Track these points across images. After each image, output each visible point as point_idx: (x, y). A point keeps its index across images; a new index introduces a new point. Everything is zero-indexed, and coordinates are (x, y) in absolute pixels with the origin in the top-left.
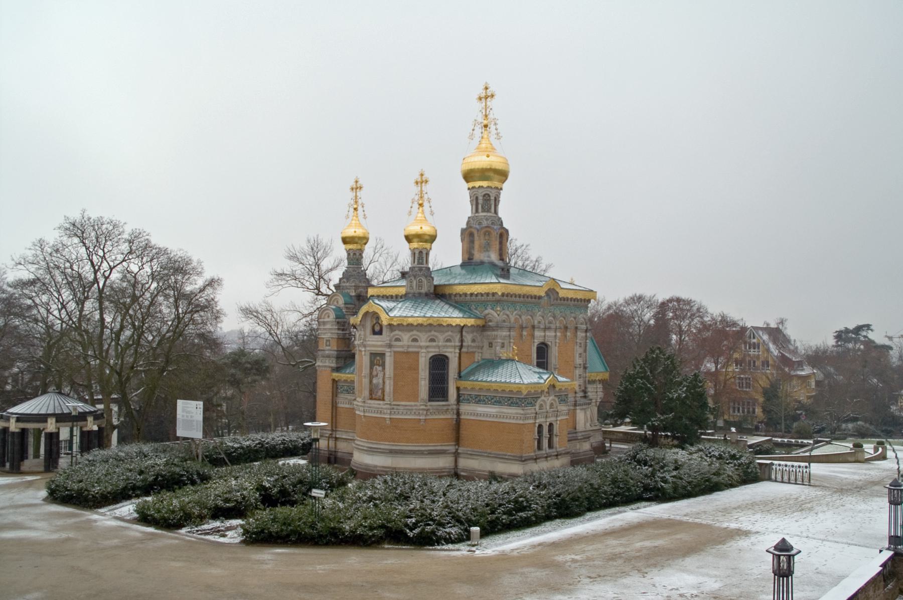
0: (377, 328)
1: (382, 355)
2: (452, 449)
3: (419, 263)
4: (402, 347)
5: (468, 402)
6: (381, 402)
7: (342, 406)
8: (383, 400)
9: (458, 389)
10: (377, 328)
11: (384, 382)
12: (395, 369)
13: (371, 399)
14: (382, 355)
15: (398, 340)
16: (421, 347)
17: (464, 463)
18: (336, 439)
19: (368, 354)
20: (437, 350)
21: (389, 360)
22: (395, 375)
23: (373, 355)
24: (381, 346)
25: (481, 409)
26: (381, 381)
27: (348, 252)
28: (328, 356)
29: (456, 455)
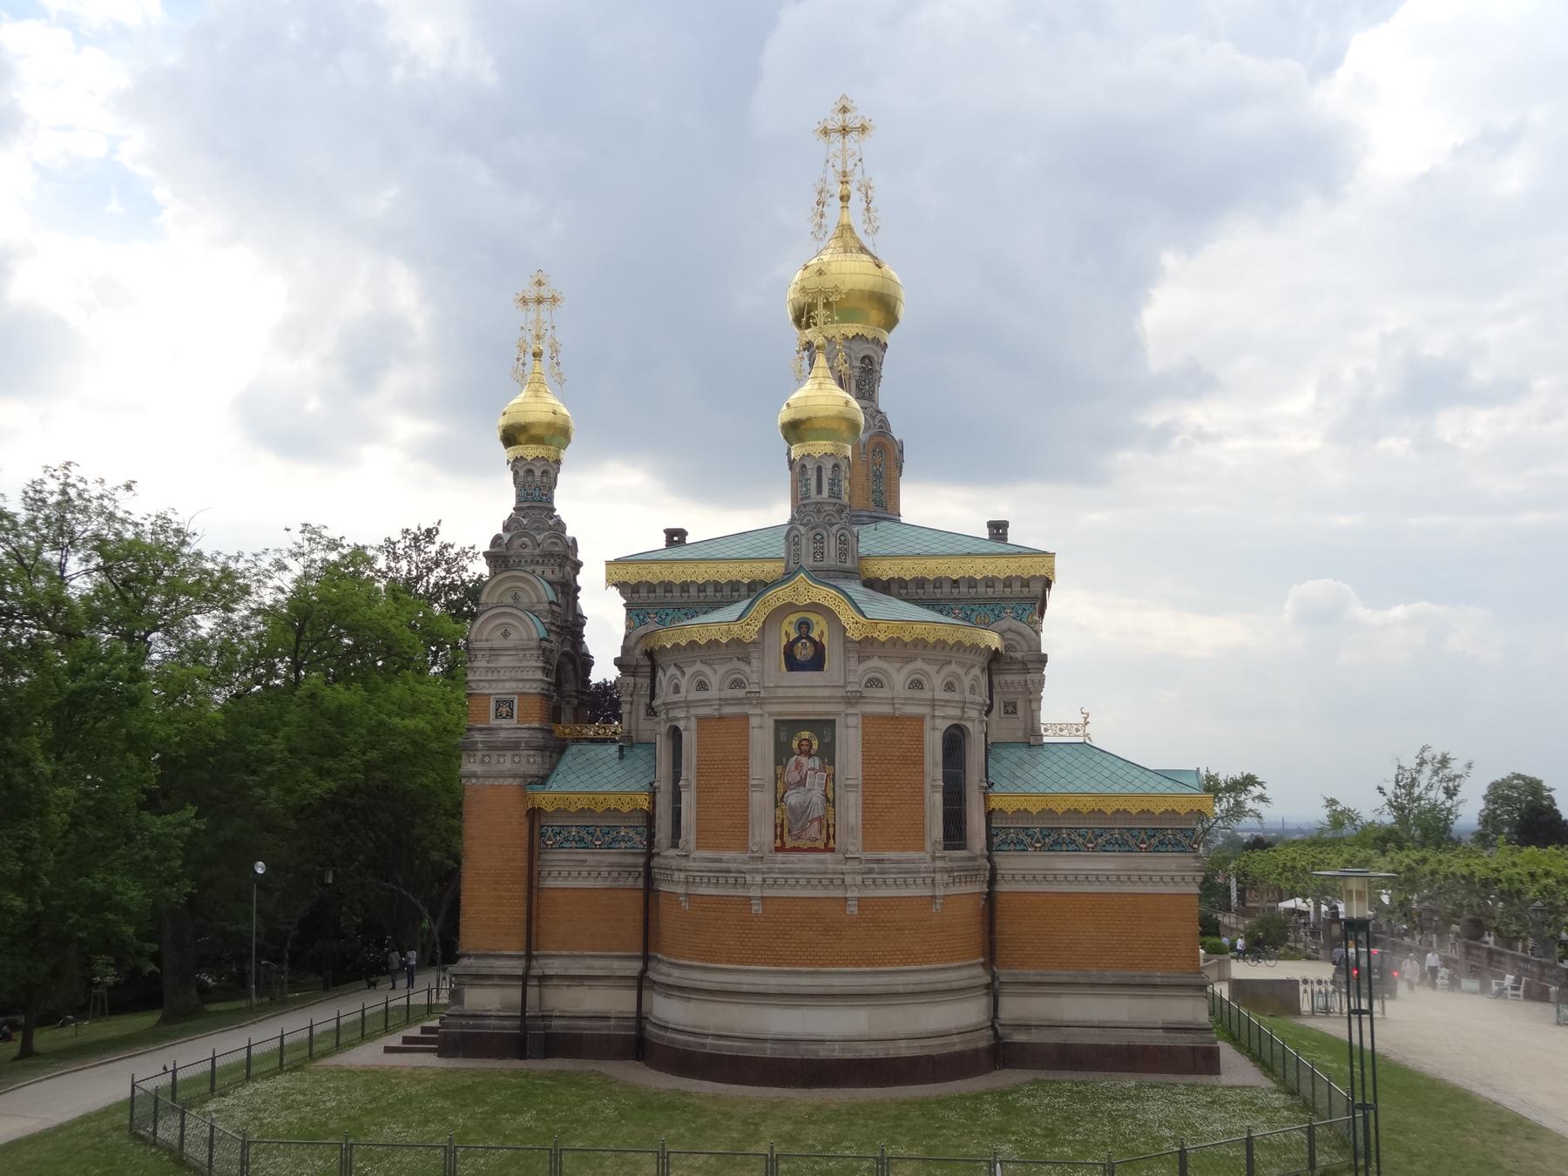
0: (804, 652)
1: (823, 727)
2: (980, 976)
3: (833, 494)
5: (1020, 846)
6: (828, 856)
7: (561, 883)
8: (828, 849)
9: (989, 815)
10: (804, 652)
11: (830, 802)
12: (866, 762)
13: (781, 849)
14: (823, 727)
15: (874, 683)
16: (933, 703)
17: (1014, 1007)
18: (543, 978)
20: (958, 713)
22: (866, 779)
23: (786, 728)
24: (828, 700)
26: (817, 797)
27: (516, 463)
28: (513, 746)
29: (993, 991)
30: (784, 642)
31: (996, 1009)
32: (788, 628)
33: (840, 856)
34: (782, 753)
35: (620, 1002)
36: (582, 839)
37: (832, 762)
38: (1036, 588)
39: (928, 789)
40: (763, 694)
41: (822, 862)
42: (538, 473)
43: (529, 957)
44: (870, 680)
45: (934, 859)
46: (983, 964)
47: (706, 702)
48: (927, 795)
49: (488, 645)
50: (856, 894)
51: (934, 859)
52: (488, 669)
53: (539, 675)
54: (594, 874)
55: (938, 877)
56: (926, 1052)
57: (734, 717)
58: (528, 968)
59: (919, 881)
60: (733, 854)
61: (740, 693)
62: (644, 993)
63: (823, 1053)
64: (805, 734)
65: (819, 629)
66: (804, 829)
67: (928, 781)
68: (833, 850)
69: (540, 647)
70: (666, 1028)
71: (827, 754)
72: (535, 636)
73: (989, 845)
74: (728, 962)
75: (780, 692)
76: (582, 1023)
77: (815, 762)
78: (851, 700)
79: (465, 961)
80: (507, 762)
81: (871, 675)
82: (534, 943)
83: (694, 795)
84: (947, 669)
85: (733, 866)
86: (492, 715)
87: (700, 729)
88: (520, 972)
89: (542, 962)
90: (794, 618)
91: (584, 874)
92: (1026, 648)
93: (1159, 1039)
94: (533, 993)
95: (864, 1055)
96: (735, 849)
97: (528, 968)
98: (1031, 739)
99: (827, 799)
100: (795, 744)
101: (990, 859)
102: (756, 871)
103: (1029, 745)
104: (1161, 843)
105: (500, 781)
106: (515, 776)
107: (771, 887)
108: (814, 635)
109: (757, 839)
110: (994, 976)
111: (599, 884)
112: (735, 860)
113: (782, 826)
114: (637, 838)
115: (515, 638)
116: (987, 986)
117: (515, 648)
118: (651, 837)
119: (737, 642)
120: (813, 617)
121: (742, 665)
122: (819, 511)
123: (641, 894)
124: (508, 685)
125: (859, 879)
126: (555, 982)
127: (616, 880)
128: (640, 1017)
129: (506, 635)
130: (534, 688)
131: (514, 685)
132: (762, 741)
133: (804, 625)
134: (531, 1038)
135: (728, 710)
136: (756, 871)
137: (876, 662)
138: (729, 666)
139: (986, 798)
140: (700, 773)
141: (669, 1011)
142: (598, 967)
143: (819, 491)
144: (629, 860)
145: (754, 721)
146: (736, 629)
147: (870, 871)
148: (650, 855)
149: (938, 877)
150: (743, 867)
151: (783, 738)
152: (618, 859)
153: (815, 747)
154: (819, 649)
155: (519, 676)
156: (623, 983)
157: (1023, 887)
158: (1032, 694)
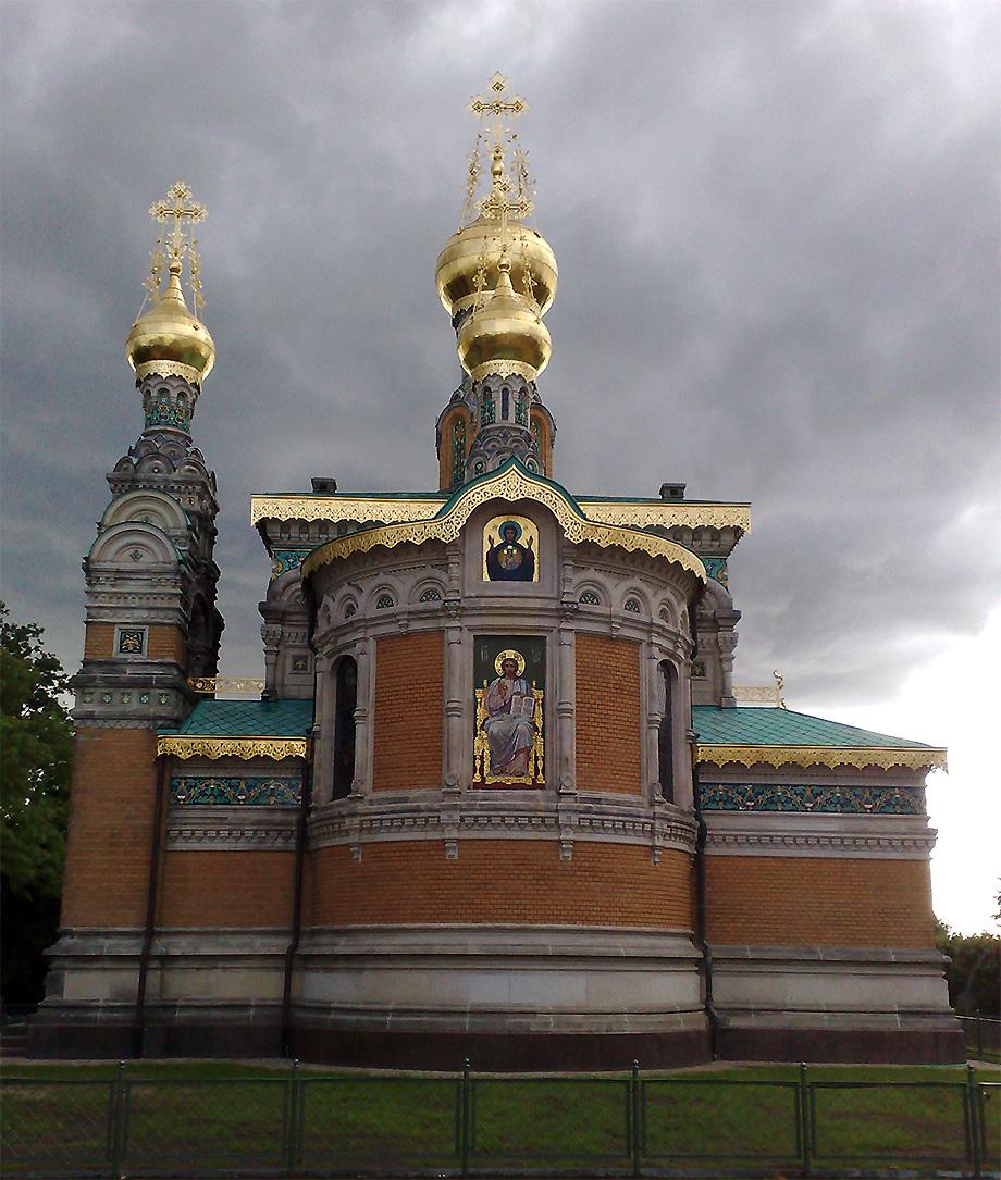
1: (532, 645)
4: (608, 619)
5: (730, 804)
7: (195, 846)
8: (535, 786)
9: (697, 769)
10: (510, 558)
14: (532, 645)
15: (589, 597)
16: (649, 628)
17: (728, 988)
18: (167, 960)
19: (469, 638)
21: (564, 660)
25: (780, 824)
26: (522, 725)
28: (143, 685)
29: (704, 968)
30: (487, 547)
31: (709, 989)
32: (492, 531)
33: (553, 793)
34: (483, 672)
35: (263, 987)
36: (222, 793)
37: (541, 686)
38: (727, 539)
39: (645, 724)
40: (463, 604)
41: (533, 798)
42: (174, 394)
43: (150, 935)
44: (584, 595)
45: (652, 804)
46: (691, 938)
47: (392, 618)
48: (644, 732)
49: (115, 566)
50: (572, 836)
51: (652, 804)
52: (112, 595)
53: (177, 604)
54: (236, 834)
55: (658, 823)
56: (651, 1029)
57: (425, 632)
58: (148, 946)
59: (639, 827)
60: (423, 791)
61: (437, 605)
62: (295, 976)
63: (535, 1025)
64: (510, 654)
65: (529, 532)
66: (507, 762)
67: (644, 718)
68: (542, 787)
69: (178, 572)
70: (329, 1010)
71: (536, 675)
72: (174, 558)
73: (696, 802)
74: (413, 921)
75: (483, 603)
76: (216, 1014)
77: (522, 686)
78: (567, 612)
79: (66, 941)
80: (132, 702)
81: (586, 588)
82: (156, 917)
83: (371, 728)
84: (661, 595)
85: (423, 804)
86: (116, 647)
87: (380, 652)
88: (137, 951)
89: (165, 940)
90: (499, 521)
91: (224, 834)
92: (715, 606)
93: (897, 1024)
94: (153, 978)
95: (584, 1030)
96: (424, 786)
97: (148, 946)
98: (722, 702)
99: (536, 729)
100: (498, 665)
101: (697, 816)
102: (455, 807)
103: (720, 708)
104: (888, 803)
105: (124, 723)
106: (142, 718)
107: (469, 827)
108: (522, 541)
109: (454, 772)
110: (705, 950)
111: (241, 846)
112: (425, 798)
113: (482, 758)
114: (289, 793)
115: (146, 561)
116: (697, 962)
117: (148, 571)
118: (306, 792)
119: (434, 544)
120: (522, 522)
121: (437, 573)
122: (505, 436)
123: (293, 857)
124: (138, 613)
125: (575, 819)
126: (182, 964)
127: (262, 841)
128: (288, 1003)
129: (135, 557)
130: (174, 618)
131: (145, 614)
132: (461, 656)
133: (511, 532)
134: (147, 1031)
135: (416, 626)
136: (455, 807)
137: (591, 574)
138: (421, 574)
139: (693, 750)
140: (380, 703)
141: (330, 989)
142: (235, 946)
143: (505, 417)
144: (278, 816)
145: (453, 636)
146: (434, 531)
147: (588, 811)
148: (306, 809)
149: (658, 823)
150: (436, 806)
151: (484, 656)
152: (264, 816)
153: (522, 668)
154: (527, 555)
155: (152, 603)
156: (269, 963)
157: (734, 851)
158: (722, 653)
